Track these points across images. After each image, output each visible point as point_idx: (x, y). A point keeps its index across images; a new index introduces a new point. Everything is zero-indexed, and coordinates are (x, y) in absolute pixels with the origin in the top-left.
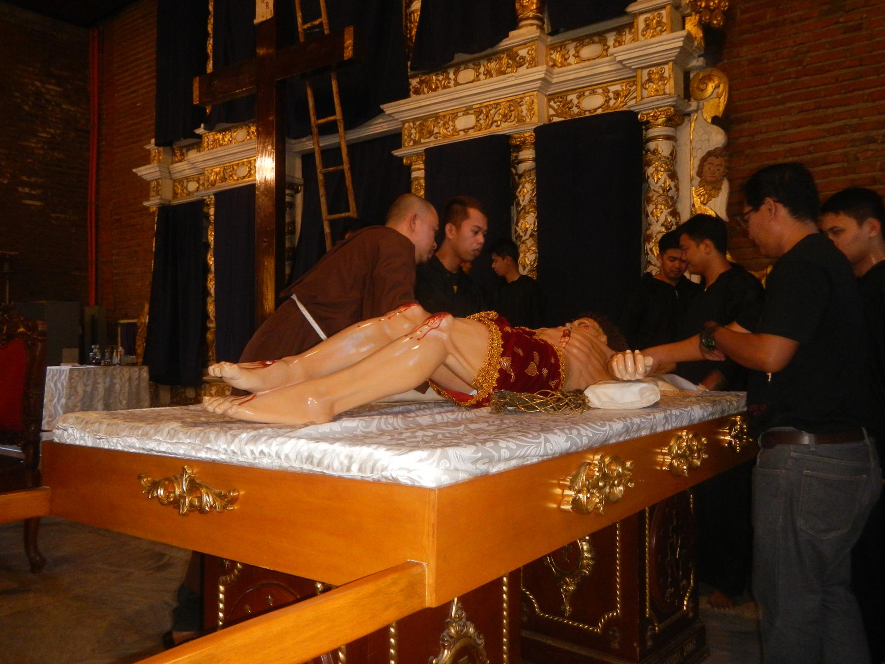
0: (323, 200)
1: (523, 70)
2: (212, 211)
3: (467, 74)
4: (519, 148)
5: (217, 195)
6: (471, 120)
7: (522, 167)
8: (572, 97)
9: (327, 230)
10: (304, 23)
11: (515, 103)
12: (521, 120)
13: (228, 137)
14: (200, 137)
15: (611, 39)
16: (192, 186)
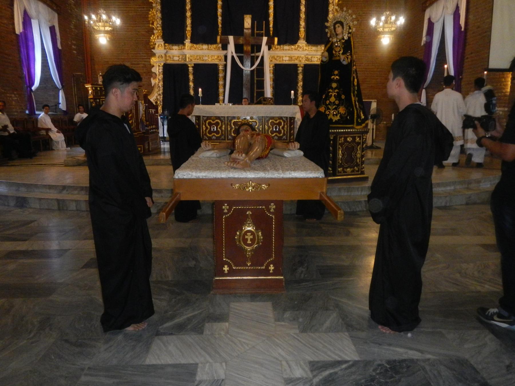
0: (255, 75)
1: (301, 50)
2: (191, 69)
3: (286, 47)
4: (298, 67)
5: (194, 64)
6: (287, 59)
7: (299, 72)
8: (310, 57)
9: (255, 82)
10: (257, 30)
11: (298, 57)
12: (300, 61)
13: (198, 46)
14: (184, 44)
15: (319, 47)
16: (176, 58)
